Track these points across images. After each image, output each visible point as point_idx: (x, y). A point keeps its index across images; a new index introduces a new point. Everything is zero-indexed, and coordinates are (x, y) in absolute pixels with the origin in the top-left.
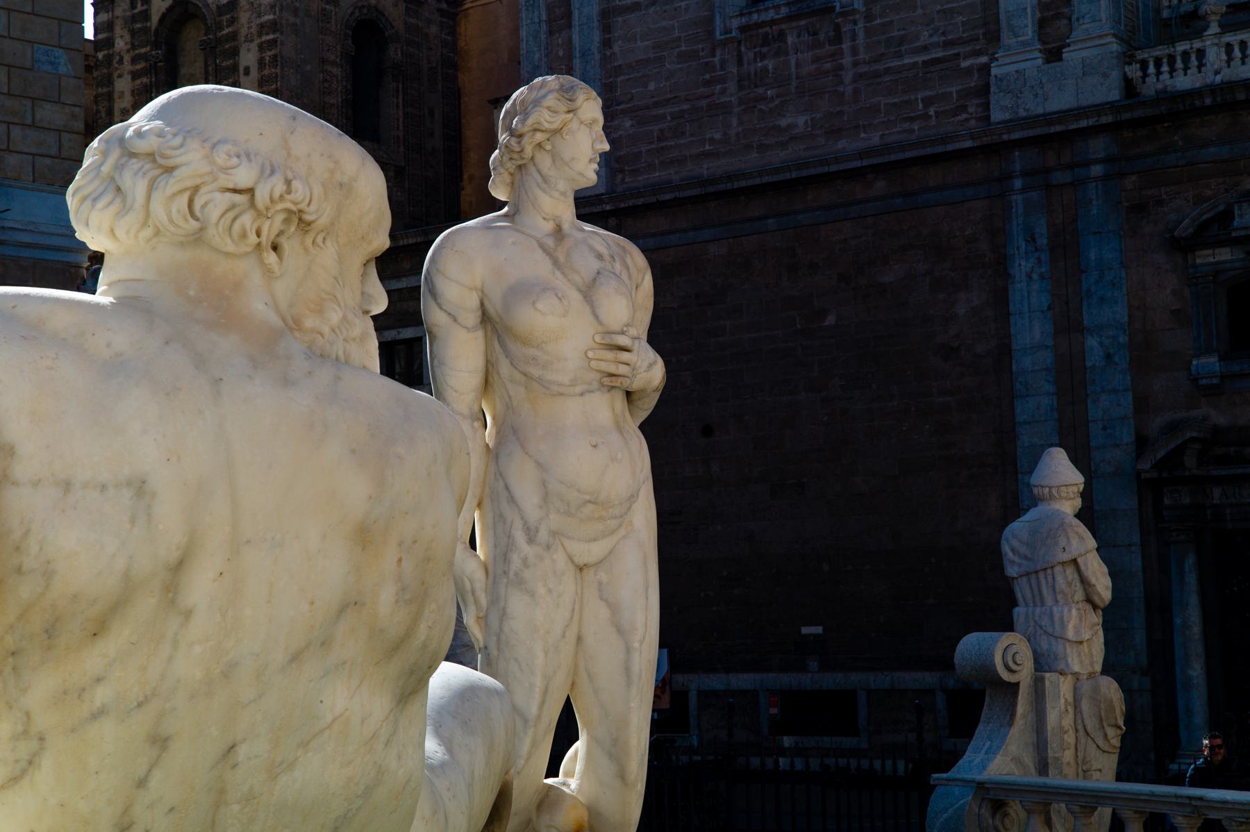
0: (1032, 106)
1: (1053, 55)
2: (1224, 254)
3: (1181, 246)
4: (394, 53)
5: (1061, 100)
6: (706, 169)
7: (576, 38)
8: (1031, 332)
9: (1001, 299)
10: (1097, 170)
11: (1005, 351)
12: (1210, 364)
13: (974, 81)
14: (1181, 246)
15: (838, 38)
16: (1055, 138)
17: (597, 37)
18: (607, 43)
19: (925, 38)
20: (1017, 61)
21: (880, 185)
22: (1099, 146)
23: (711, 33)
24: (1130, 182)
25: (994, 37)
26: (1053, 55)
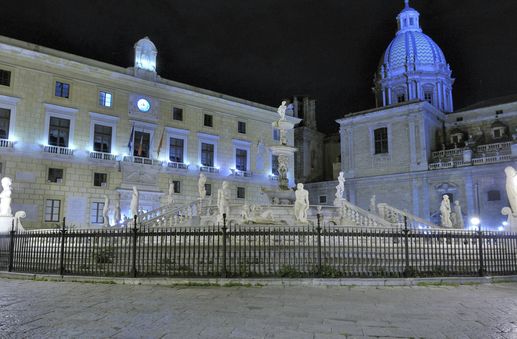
1: (418, 164)
4: (316, 155)
9: (411, 194)
10: (425, 179)
11: (412, 201)
13: (408, 166)
19: (401, 160)
24: (429, 180)
26: (418, 164)
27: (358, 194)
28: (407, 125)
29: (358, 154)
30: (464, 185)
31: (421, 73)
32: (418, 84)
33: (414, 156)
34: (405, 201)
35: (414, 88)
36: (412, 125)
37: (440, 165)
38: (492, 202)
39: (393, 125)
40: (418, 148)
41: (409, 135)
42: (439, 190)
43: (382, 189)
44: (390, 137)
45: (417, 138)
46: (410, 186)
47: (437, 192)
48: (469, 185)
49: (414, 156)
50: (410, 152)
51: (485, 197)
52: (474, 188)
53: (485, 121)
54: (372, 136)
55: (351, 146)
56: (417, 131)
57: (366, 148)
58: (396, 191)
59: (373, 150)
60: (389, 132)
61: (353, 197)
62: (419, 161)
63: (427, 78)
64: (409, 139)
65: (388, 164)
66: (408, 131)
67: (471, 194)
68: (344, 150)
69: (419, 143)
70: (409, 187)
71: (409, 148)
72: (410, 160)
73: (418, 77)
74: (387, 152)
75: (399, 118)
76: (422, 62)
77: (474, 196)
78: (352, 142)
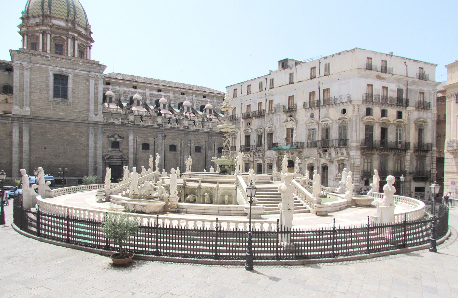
0: (93, 120)
1: (96, 115)
2: (112, 139)
5: (97, 120)
7: (25, 93)
8: (91, 143)
9: (88, 139)
11: (88, 145)
12: (110, 149)
13: (86, 115)
15: (68, 105)
16: (96, 124)
17: (29, 95)
18: (30, 96)
19: (80, 109)
21: (73, 124)
22: (100, 126)
23: (48, 100)
26: (96, 115)
28: (88, 81)
29: (36, 92)
30: (128, 137)
31: (79, 33)
32: (77, 42)
33: (92, 107)
34: (81, 144)
35: (72, 44)
36: (92, 82)
37: (112, 120)
38: (144, 151)
39: (74, 76)
40: (96, 102)
41: (88, 90)
42: (111, 139)
43: (60, 131)
44: (70, 85)
45: (96, 94)
46: (87, 132)
47: (109, 140)
49: (92, 107)
50: (89, 104)
51: (141, 147)
52: (134, 140)
53: (126, 91)
55: (27, 82)
56: (96, 88)
57: (45, 90)
59: (51, 93)
62: (96, 113)
63: (81, 39)
64: (89, 93)
65: (68, 109)
66: (89, 86)
67: (132, 144)
68: (18, 85)
69: (98, 98)
70: (86, 133)
72: (88, 110)
73: (77, 35)
74: (67, 98)
75: (81, 72)
76: (81, 24)
77: (134, 146)
78: (29, 80)
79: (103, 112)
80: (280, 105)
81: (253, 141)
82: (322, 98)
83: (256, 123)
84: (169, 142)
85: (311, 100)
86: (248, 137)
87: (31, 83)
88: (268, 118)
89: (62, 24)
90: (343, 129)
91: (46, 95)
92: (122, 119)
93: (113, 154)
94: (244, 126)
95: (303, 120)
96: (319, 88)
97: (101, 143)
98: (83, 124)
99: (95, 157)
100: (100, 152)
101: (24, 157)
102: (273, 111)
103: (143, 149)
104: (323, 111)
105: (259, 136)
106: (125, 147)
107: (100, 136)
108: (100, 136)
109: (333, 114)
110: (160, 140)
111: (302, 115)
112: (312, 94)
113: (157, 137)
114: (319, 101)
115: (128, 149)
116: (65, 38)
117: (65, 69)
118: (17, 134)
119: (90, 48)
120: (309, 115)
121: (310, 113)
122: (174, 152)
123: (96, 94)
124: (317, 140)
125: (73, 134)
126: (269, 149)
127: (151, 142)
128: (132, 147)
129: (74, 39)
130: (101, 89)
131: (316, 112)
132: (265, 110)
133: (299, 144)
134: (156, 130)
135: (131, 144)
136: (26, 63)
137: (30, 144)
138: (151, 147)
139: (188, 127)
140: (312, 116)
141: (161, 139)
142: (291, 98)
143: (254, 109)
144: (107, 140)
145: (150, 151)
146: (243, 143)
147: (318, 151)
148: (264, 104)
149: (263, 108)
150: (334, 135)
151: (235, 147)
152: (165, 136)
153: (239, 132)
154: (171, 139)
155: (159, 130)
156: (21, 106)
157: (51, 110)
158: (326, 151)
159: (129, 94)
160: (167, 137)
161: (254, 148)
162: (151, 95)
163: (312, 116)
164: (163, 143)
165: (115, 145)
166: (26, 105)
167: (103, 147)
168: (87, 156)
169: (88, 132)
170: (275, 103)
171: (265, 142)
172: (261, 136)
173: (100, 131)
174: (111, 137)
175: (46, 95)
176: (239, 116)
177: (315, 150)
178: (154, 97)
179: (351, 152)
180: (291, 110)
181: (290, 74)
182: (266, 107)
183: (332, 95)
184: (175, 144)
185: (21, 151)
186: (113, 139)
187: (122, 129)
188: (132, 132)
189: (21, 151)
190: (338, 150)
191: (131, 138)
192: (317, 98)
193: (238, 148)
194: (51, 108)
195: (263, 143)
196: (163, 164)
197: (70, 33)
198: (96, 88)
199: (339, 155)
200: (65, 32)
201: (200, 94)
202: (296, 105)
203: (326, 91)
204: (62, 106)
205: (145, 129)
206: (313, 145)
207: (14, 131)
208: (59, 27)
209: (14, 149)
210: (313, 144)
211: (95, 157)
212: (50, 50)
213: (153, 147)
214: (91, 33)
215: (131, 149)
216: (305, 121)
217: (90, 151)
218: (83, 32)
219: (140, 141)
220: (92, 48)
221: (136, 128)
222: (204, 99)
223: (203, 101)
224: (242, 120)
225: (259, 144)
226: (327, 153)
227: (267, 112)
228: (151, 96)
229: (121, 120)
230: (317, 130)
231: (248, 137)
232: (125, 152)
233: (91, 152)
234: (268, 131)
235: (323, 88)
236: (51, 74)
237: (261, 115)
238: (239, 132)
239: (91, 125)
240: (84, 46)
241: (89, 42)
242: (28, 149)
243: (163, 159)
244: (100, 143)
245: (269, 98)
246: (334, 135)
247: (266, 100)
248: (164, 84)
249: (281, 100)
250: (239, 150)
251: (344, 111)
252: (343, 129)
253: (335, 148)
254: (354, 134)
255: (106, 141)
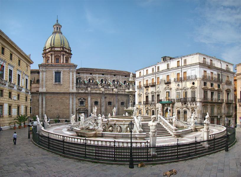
1: (73, 89)
3: (79, 99)
5: (73, 91)
6: (52, 91)
8: (71, 102)
9: (69, 101)
12: (79, 105)
14: (79, 99)
16: (73, 93)
20: (71, 88)
22: (75, 94)
25: (70, 87)
26: (73, 89)
27: (47, 99)
28: (69, 73)
31: (66, 52)
32: (64, 56)
33: (71, 86)
34: (66, 103)
36: (71, 74)
39: (63, 72)
40: (73, 83)
41: (70, 77)
44: (62, 76)
45: (73, 79)
47: (79, 101)
48: (89, 99)
49: (71, 86)
50: (70, 84)
51: (94, 104)
52: (91, 100)
54: (54, 74)
56: (73, 76)
57: (51, 79)
58: (63, 99)
59: (54, 80)
60: (61, 74)
61: (45, 100)
63: (67, 54)
64: (70, 79)
66: (69, 75)
67: (90, 102)
68: (41, 79)
69: (73, 81)
71: (70, 82)
72: (69, 87)
79: (76, 87)
80: (163, 80)
81: (150, 99)
82: (183, 76)
83: (151, 89)
84: (108, 100)
85: (178, 77)
86: (147, 97)
87: (46, 78)
88: (157, 87)
89: (59, 49)
90: (193, 93)
91: (52, 82)
92: (85, 90)
93: (81, 107)
94: (145, 91)
95: (174, 88)
96: (181, 72)
97: (75, 102)
98: (67, 94)
99: (73, 109)
100: (75, 106)
101: (43, 110)
102: (159, 83)
103: (95, 104)
104: (184, 83)
105: (153, 96)
106: (86, 104)
107: (75, 99)
108: (75, 99)
109: (189, 85)
110: (103, 100)
111: (173, 86)
112: (178, 74)
113: (102, 98)
114: (181, 78)
115: (88, 105)
116: (60, 55)
117: (59, 69)
118: (41, 100)
119: (71, 58)
120: (177, 85)
121: (178, 84)
122: (110, 105)
123: (73, 79)
124: (181, 98)
125: (63, 99)
126: (158, 102)
127: (99, 100)
128: (90, 104)
129: (63, 55)
130: (75, 76)
131: (180, 84)
132: (156, 83)
133: (173, 100)
134: (101, 95)
135: (89, 102)
136: (44, 69)
137: (46, 104)
138: (99, 103)
139: (117, 92)
140: (178, 85)
141: (104, 99)
142: (168, 76)
143: (150, 82)
144: (78, 101)
145: (98, 105)
146: (145, 100)
147: (182, 103)
148: (155, 79)
149: (155, 82)
150: (189, 96)
151: (141, 102)
152: (106, 98)
153: (143, 94)
154: (109, 99)
155: (103, 95)
156: (43, 88)
157: (53, 88)
158: (186, 103)
159: (88, 77)
160: (107, 98)
161: (150, 103)
162: (99, 77)
163: (178, 85)
164: (105, 101)
165: (82, 103)
166: (44, 87)
167: (76, 104)
168: (69, 109)
169: (69, 97)
170: (160, 78)
171: (156, 99)
172: (154, 95)
173: (74, 97)
174: (80, 99)
175: (52, 82)
176: (143, 86)
177: (181, 103)
178: (100, 78)
179: (197, 104)
180: (168, 83)
181: (167, 64)
182: (156, 81)
183: (188, 75)
184: (111, 101)
185: (42, 108)
186: (81, 100)
187: (85, 95)
188: (89, 96)
189: (42, 108)
190: (191, 103)
191: (89, 99)
192: (180, 76)
193: (142, 103)
194: (54, 87)
195: (155, 100)
196: (105, 112)
197: (62, 53)
198: (73, 76)
199: (192, 105)
200: (60, 53)
201: (124, 75)
202: (171, 80)
203: (185, 73)
204: (58, 86)
205: (96, 95)
206: (179, 101)
207: (40, 99)
208: (58, 51)
209: (40, 107)
210: (179, 100)
211: (73, 109)
212: (54, 62)
213: (100, 103)
214: (71, 51)
215: (89, 105)
216: (175, 88)
217: (70, 106)
218: (68, 51)
219: (94, 100)
220: (71, 58)
221: (91, 94)
222: (126, 78)
223: (125, 79)
224: (144, 88)
225: (153, 100)
226: (186, 105)
227: (156, 83)
228: (99, 78)
229: (84, 91)
230: (181, 93)
231: (147, 97)
232: (86, 106)
233: (71, 107)
234: (157, 94)
235: (183, 71)
236: (54, 72)
237: (153, 86)
238: (143, 94)
239: (71, 94)
240: (68, 57)
241: (70, 55)
242: (45, 106)
243: (105, 109)
244: (75, 102)
245: (157, 77)
246: (189, 96)
247: (156, 77)
248: (105, 71)
249: (163, 77)
250: (143, 104)
251: (193, 83)
252: (193, 93)
253: (190, 102)
254: (199, 95)
255: (77, 101)
